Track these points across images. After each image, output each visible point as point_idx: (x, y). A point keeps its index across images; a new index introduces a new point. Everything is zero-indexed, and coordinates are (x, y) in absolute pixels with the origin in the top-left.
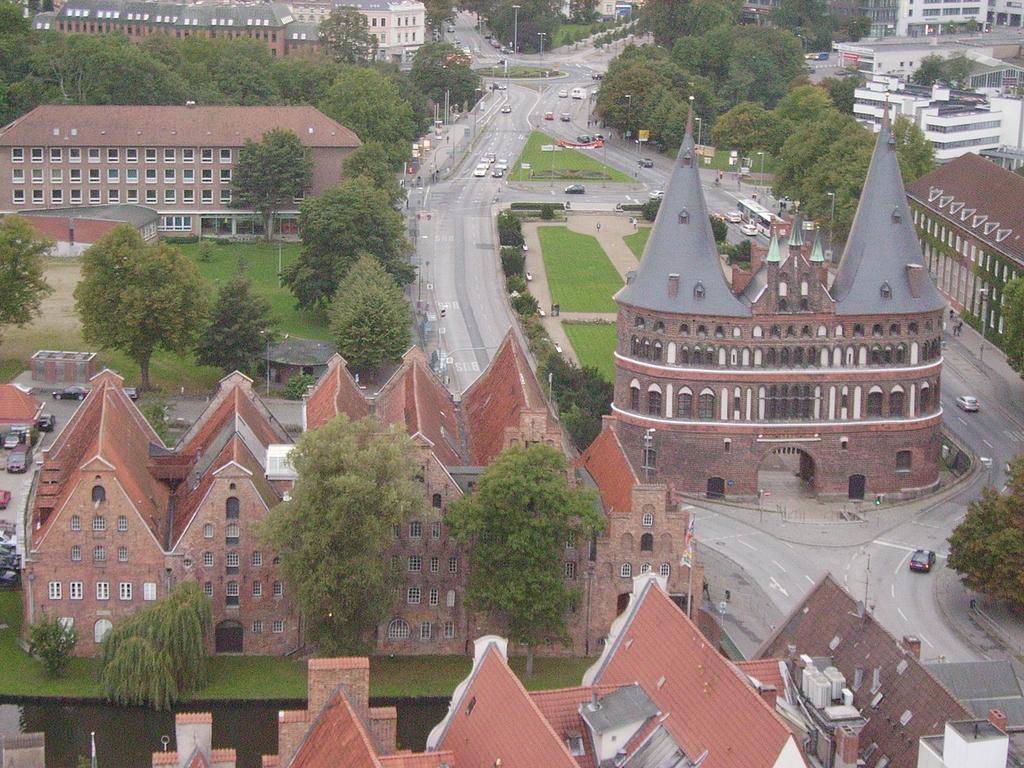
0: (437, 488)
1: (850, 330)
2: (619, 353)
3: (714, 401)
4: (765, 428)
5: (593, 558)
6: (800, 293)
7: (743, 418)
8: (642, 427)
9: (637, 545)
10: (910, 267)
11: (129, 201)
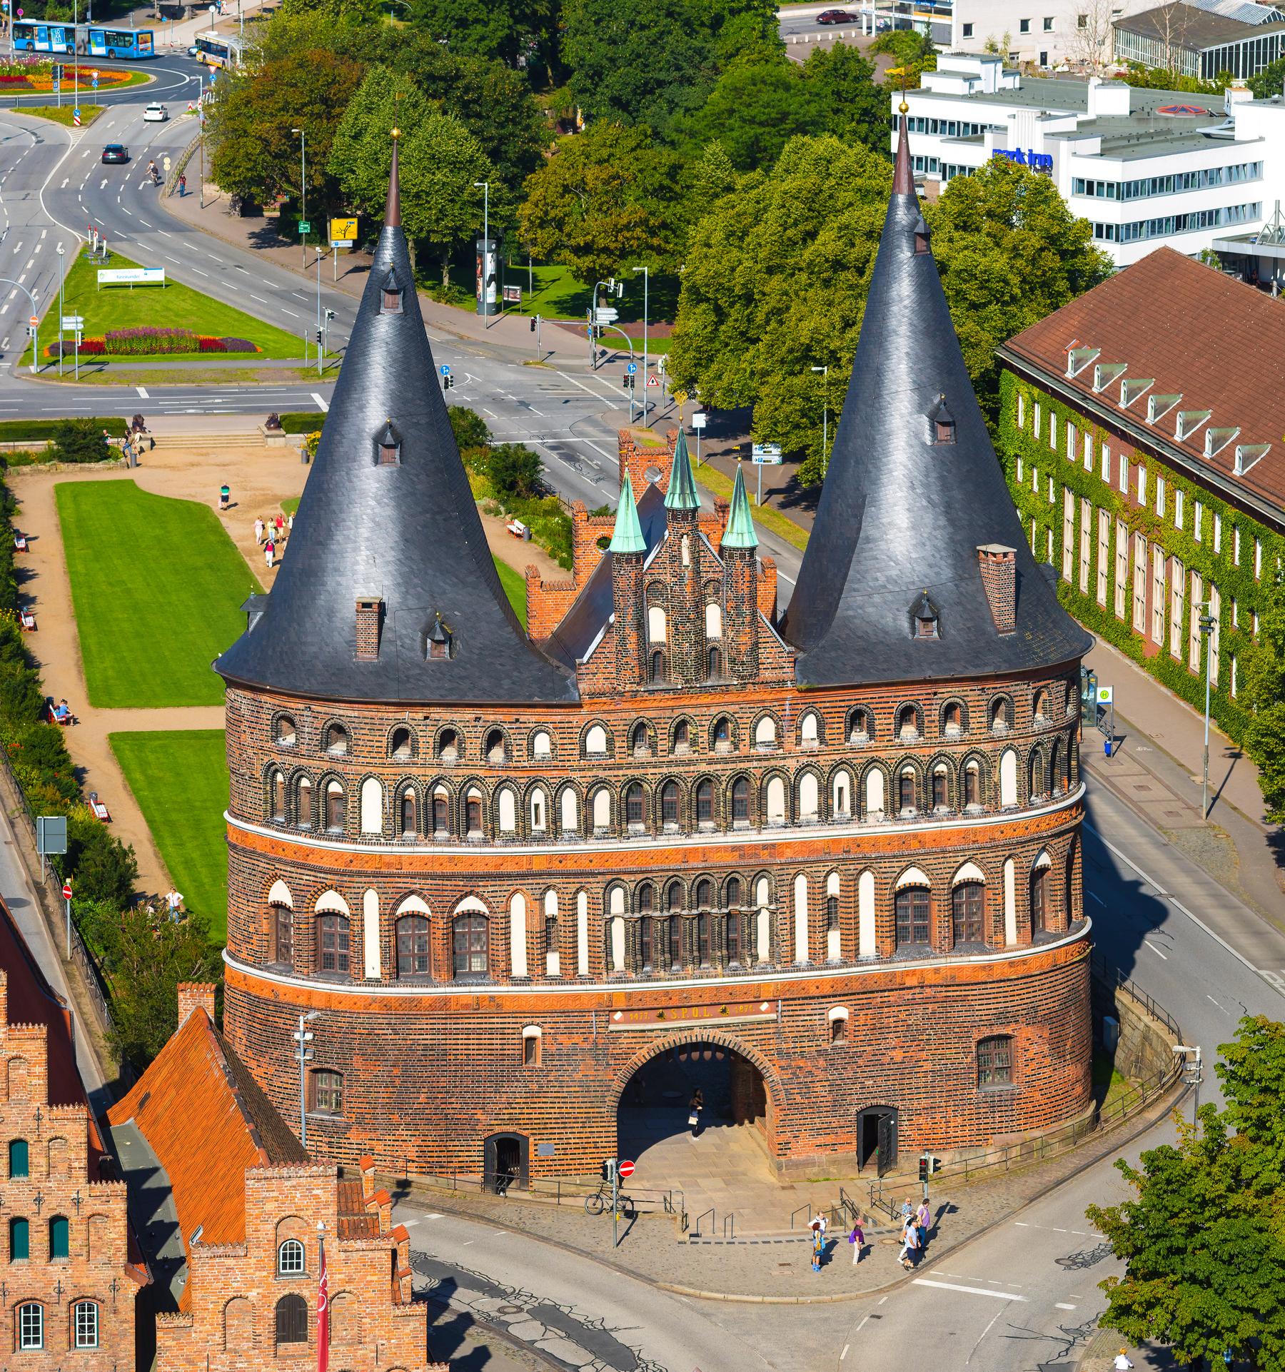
1: (837, 726)
2: (236, 816)
3: (492, 926)
4: (629, 996)
6: (701, 631)
7: (570, 972)
8: (290, 1009)
9: (266, 1328)
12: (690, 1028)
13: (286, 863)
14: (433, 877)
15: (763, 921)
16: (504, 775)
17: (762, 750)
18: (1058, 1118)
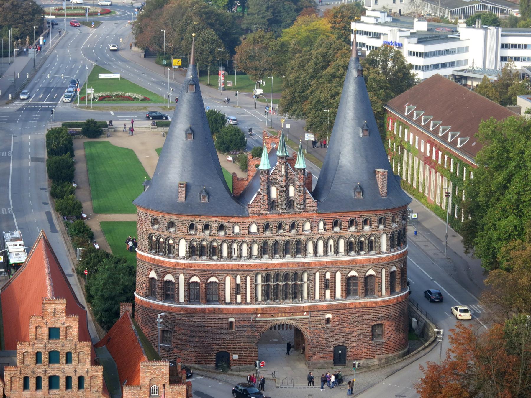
1: (330, 225)
2: (140, 250)
4: (263, 309)
6: (287, 194)
10: (378, 171)
12: (282, 320)
13: (155, 265)
14: (202, 270)
16: (224, 238)
17: (306, 232)
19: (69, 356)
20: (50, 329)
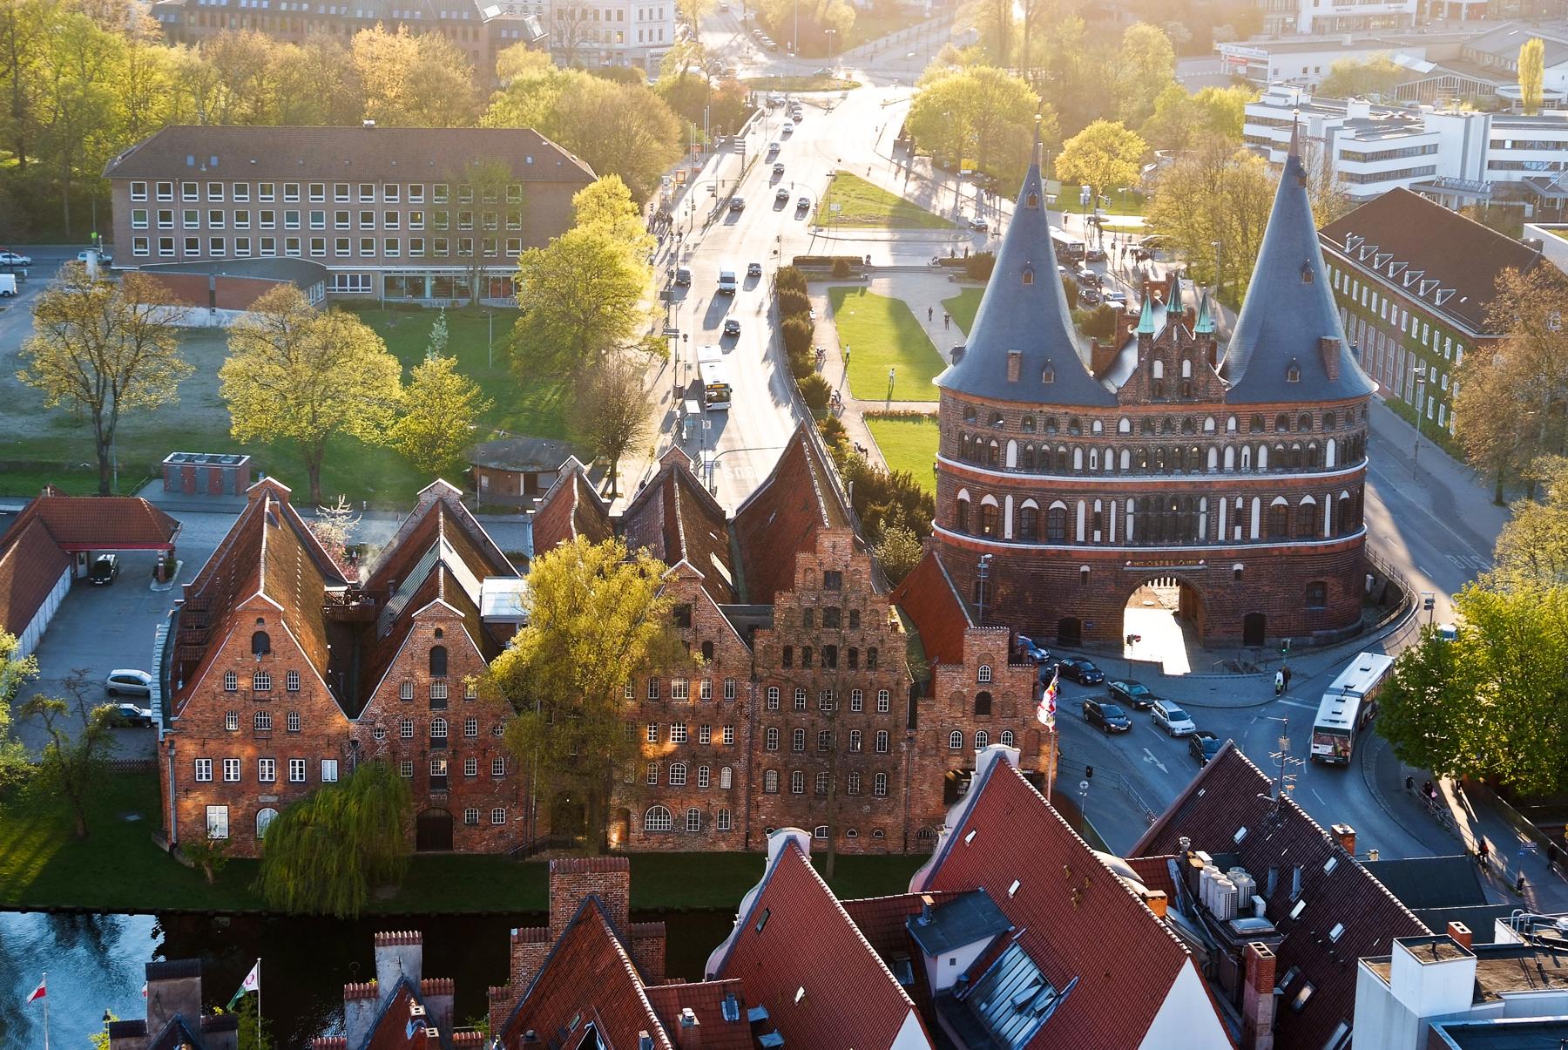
0: (708, 634)
1: (1246, 423)
3: (1068, 516)
5: (913, 725)
8: (977, 552)
11: (288, 254)
15: (1203, 518)
18: (1345, 625)
19: (855, 614)
20: (826, 573)
